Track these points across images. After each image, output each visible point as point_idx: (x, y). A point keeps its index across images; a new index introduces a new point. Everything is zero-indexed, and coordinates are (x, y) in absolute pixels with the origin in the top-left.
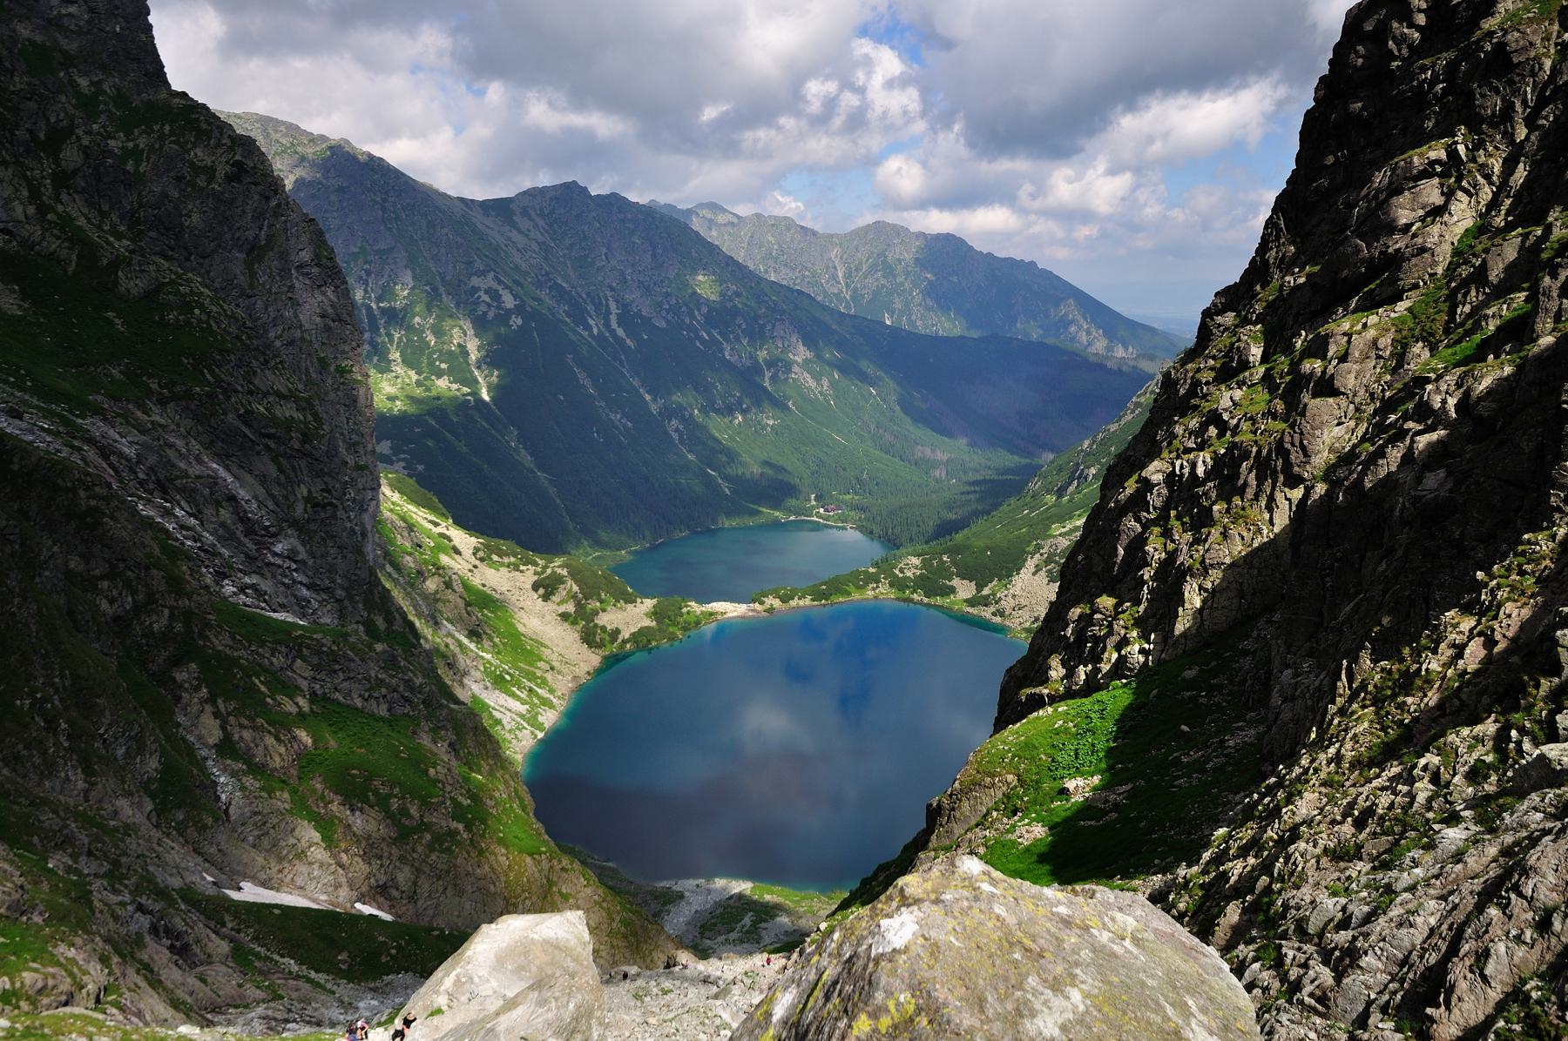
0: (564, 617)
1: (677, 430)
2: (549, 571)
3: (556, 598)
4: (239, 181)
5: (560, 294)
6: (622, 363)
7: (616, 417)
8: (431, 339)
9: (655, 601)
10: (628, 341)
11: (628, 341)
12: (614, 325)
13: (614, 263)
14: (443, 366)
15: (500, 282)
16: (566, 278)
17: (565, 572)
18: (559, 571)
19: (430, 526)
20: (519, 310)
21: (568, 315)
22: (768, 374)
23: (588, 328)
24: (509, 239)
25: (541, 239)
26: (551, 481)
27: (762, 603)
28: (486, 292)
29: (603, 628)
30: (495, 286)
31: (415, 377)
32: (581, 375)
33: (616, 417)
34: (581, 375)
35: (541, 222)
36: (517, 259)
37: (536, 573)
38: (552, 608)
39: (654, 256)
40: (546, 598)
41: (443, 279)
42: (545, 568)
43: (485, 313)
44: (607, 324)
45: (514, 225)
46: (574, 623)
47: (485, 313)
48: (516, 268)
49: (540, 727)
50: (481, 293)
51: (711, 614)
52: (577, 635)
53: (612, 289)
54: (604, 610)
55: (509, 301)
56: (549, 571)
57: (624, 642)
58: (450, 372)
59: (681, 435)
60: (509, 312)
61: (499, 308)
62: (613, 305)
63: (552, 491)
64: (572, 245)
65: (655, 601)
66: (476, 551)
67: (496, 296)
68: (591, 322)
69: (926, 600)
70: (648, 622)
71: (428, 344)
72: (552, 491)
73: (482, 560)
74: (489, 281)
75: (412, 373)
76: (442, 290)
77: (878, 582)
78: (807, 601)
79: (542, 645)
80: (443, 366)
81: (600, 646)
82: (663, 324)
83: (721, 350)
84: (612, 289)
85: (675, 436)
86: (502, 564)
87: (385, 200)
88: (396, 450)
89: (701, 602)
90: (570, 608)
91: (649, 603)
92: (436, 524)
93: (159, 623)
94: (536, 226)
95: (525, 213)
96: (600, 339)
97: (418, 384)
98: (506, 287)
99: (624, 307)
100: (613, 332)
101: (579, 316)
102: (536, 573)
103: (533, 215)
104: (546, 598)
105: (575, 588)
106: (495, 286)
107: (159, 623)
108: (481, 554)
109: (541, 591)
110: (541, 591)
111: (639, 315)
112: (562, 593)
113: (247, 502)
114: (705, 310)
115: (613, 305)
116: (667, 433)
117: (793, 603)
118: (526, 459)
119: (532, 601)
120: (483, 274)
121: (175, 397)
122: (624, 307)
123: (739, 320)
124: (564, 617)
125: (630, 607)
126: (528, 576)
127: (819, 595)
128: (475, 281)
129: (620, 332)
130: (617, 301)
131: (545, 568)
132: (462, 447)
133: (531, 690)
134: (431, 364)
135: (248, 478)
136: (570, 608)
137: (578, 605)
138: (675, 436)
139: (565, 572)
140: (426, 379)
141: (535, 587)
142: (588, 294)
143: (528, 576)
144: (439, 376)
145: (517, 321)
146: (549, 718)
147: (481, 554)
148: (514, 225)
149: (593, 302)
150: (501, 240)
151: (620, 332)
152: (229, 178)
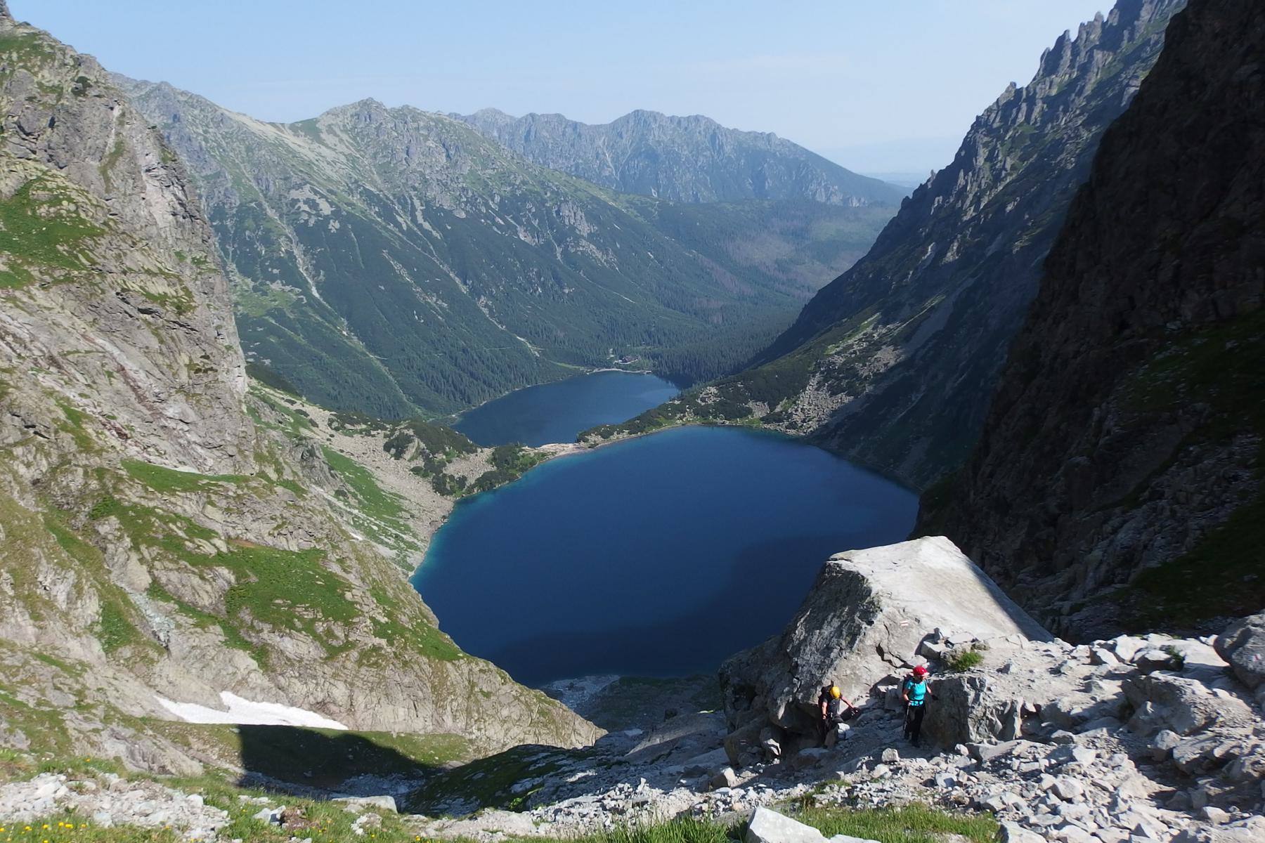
0: (416, 471)
1: (487, 305)
2: (397, 433)
3: (407, 456)
4: (85, 95)
5: (369, 197)
6: (431, 253)
7: (432, 300)
9: (492, 450)
10: (434, 233)
11: (434, 233)
13: (413, 166)
14: (276, 271)
15: (316, 193)
16: (373, 182)
17: (411, 432)
18: (406, 431)
19: (288, 405)
20: (336, 214)
21: (380, 216)
22: (559, 250)
23: (398, 225)
24: (319, 154)
25: (347, 151)
26: (382, 362)
27: (586, 441)
28: (305, 203)
29: (452, 477)
30: (312, 196)
31: (252, 284)
32: (398, 267)
33: (432, 300)
34: (398, 267)
35: (345, 137)
36: (328, 171)
37: (386, 436)
38: (406, 463)
39: (448, 156)
40: (398, 456)
41: (265, 196)
42: (393, 430)
43: (306, 221)
44: (414, 220)
45: (321, 142)
46: (425, 476)
47: (306, 221)
48: (329, 179)
49: (410, 568)
50: (301, 204)
51: (544, 455)
52: (430, 486)
53: (415, 189)
54: (450, 462)
55: (326, 209)
56: (397, 433)
57: (473, 487)
60: (327, 218)
61: (318, 215)
62: (417, 203)
63: (384, 370)
64: (376, 154)
65: (492, 450)
66: (330, 422)
67: (313, 204)
68: (399, 219)
69: (727, 423)
70: (491, 468)
71: (259, 254)
72: (384, 370)
73: (336, 429)
74: (306, 193)
75: (249, 281)
76: (266, 205)
77: (684, 412)
78: (625, 435)
79: (401, 497)
80: (276, 271)
81: (450, 493)
82: (463, 215)
83: (516, 233)
84: (415, 189)
85: (485, 311)
86: (356, 432)
87: (206, 132)
89: (533, 446)
90: (420, 463)
91: (488, 452)
92: (293, 403)
93: (76, 481)
94: (341, 141)
95: (330, 130)
96: (409, 233)
97: (255, 289)
98: (322, 196)
99: (427, 203)
100: (420, 226)
102: (386, 436)
103: (339, 132)
104: (398, 456)
105: (423, 445)
106: (312, 196)
107: (76, 481)
108: (335, 424)
109: (393, 451)
110: (393, 451)
111: (441, 209)
112: (411, 451)
113: (136, 372)
114: (497, 199)
115: (417, 203)
117: (615, 437)
118: (357, 343)
119: (388, 460)
120: (299, 187)
121: (57, 282)
122: (427, 203)
123: (529, 206)
124: (416, 471)
125: (472, 456)
126: (380, 438)
127: (633, 427)
128: (294, 194)
129: (427, 226)
130: (420, 199)
131: (393, 430)
132: (301, 339)
133: (397, 536)
134: (264, 270)
135: (134, 351)
136: (420, 463)
137: (428, 460)
138: (485, 311)
139: (411, 432)
140: (261, 284)
141: (387, 448)
142: (394, 195)
143: (380, 438)
144: (273, 282)
145: (334, 226)
146: (417, 559)
147: (335, 424)
148: (321, 142)
149: (399, 203)
150: (312, 156)
151: (427, 226)
152: (77, 92)
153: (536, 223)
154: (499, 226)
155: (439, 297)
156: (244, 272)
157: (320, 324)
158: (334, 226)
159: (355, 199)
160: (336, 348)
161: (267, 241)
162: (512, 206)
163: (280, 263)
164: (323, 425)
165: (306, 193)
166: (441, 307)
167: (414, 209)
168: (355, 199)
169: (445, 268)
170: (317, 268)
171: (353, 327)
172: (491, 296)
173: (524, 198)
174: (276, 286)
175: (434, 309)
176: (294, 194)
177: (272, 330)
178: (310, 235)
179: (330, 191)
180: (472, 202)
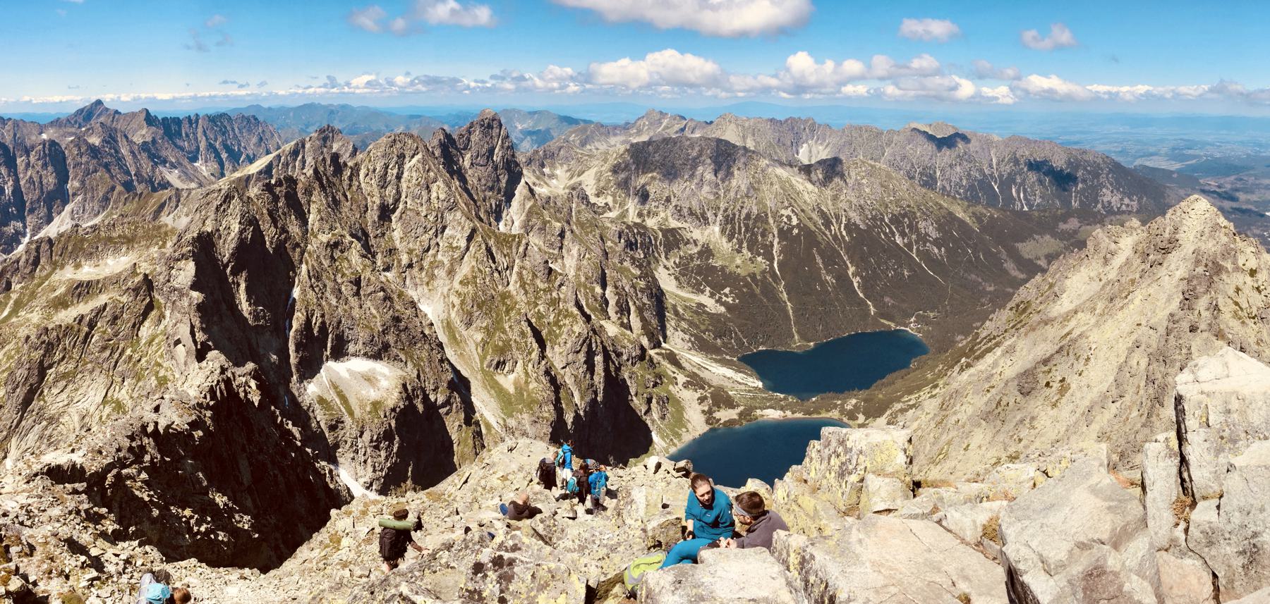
5: (823, 215)
33: (828, 278)
36: (806, 197)
55: (795, 221)
58: (763, 255)
60: (793, 227)
67: (789, 218)
74: (788, 212)
88: (731, 292)
96: (835, 237)
99: (849, 220)
101: (828, 224)
111: (855, 224)
119: (695, 404)
122: (849, 220)
128: (783, 212)
132: (758, 291)
137: (710, 409)
145: (796, 231)
150: (801, 188)
154: (885, 234)
156: (750, 249)
158: (796, 231)
159: (815, 216)
160: (775, 298)
161: (763, 235)
162: (896, 220)
163: (765, 246)
164: (680, 385)
165: (788, 212)
168: (815, 216)
171: (785, 287)
172: (861, 277)
173: (904, 216)
174: (759, 259)
176: (783, 212)
177: (747, 285)
178: (784, 234)
179: (803, 211)
180: (874, 218)
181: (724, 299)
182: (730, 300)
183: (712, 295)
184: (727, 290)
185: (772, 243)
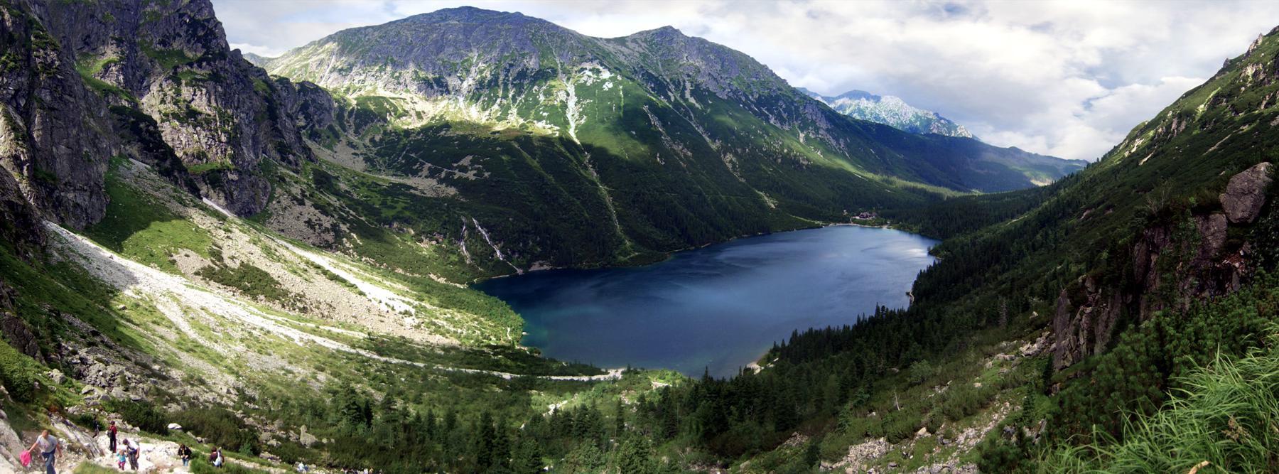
7: (678, 148)
8: (542, 98)
12: (687, 95)
16: (656, 70)
22: (802, 135)
23: (668, 98)
26: (609, 192)
33: (678, 148)
44: (683, 96)
59: (734, 166)
62: (688, 85)
63: (609, 200)
85: (730, 166)
88: (473, 162)
96: (677, 105)
100: (686, 100)
115: (688, 85)
116: (722, 163)
123: (781, 103)
134: (537, 113)
144: (539, 120)
151: (692, 100)
153: (785, 116)
155: (685, 146)
157: (560, 153)
166: (685, 155)
167: (685, 88)
169: (700, 130)
170: (581, 115)
172: (736, 154)
175: (678, 155)
181: (458, 174)
182: (471, 175)
183: (432, 174)
184: (466, 161)
185: (564, 106)
